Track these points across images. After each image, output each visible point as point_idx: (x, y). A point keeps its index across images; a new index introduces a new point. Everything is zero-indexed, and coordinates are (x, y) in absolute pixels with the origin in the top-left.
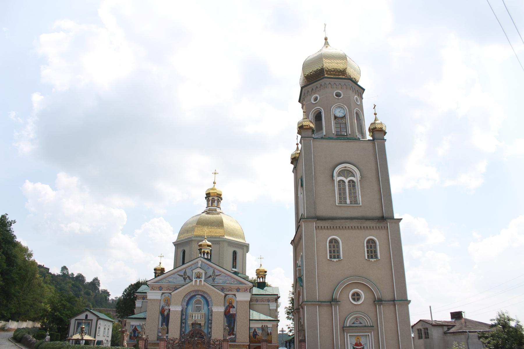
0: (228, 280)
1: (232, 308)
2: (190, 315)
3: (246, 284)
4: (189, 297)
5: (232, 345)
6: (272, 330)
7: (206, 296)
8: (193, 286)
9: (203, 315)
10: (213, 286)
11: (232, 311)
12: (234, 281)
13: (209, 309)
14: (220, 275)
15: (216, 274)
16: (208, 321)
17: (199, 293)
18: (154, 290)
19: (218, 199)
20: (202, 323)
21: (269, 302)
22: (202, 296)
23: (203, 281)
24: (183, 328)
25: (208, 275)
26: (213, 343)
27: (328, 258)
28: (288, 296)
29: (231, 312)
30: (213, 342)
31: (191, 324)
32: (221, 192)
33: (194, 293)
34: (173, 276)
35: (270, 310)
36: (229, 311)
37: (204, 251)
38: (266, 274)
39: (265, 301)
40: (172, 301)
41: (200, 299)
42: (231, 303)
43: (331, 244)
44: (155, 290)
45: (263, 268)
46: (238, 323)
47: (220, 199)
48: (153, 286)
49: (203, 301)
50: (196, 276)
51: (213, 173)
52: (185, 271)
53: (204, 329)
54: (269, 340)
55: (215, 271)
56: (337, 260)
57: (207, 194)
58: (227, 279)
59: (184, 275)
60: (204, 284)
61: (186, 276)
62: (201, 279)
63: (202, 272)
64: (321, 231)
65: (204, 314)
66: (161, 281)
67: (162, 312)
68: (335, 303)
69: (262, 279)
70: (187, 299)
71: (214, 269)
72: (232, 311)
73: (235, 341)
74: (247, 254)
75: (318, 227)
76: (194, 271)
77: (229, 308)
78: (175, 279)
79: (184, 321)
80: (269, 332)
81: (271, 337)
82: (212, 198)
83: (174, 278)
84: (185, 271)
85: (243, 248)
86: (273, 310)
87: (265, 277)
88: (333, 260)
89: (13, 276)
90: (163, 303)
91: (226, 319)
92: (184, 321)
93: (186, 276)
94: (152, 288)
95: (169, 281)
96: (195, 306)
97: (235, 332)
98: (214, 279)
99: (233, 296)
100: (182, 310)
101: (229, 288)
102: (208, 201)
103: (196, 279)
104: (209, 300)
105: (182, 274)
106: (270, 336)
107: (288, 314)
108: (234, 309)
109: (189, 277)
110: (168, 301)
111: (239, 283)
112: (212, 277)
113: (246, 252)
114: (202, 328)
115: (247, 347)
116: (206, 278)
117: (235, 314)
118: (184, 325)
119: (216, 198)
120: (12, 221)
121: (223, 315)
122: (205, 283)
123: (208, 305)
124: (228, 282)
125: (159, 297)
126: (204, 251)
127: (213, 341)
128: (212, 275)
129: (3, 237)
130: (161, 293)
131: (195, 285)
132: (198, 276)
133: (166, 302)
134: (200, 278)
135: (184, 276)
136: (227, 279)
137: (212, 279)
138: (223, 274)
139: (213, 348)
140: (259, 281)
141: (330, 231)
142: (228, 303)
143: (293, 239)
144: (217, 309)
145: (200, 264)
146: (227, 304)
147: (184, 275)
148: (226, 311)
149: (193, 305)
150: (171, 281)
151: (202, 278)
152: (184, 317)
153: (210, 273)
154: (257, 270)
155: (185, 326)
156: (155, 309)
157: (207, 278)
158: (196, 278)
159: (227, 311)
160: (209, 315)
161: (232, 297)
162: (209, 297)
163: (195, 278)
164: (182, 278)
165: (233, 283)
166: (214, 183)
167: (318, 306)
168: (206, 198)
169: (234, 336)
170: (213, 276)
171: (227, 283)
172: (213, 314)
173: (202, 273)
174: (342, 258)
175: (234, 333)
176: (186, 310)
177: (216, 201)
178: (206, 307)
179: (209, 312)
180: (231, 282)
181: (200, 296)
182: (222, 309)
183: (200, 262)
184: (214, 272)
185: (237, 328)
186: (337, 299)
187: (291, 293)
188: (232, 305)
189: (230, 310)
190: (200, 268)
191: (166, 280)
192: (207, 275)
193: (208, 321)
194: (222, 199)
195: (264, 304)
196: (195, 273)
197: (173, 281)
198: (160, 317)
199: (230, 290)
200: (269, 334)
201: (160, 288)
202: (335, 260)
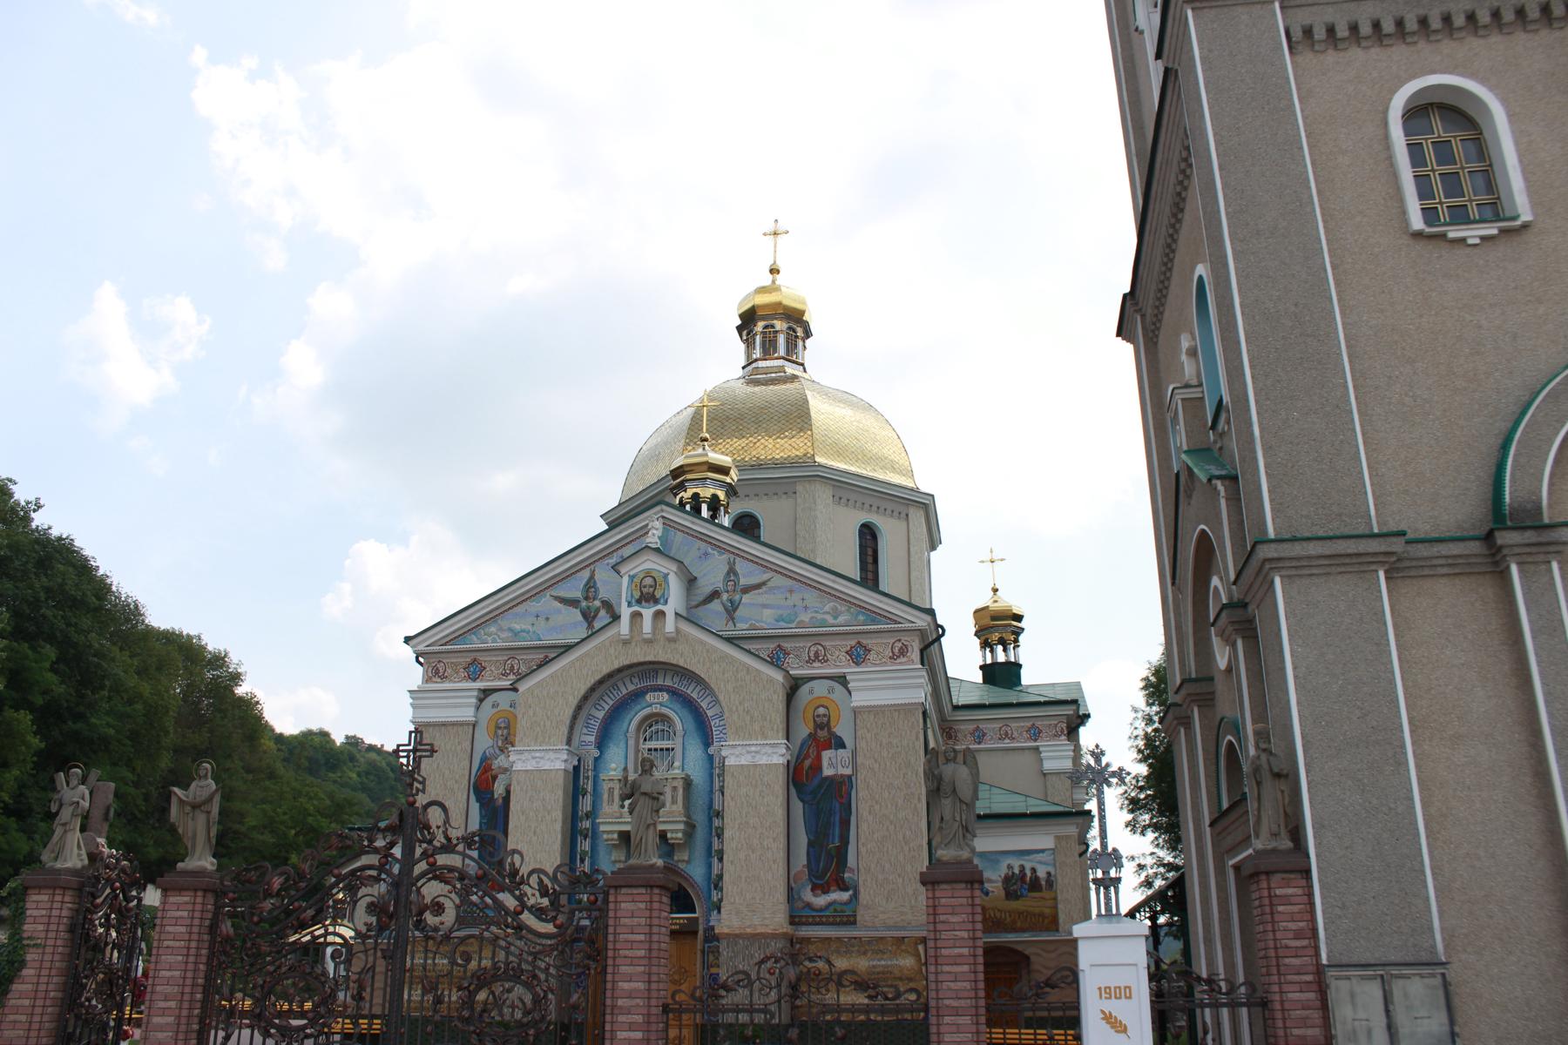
0: (806, 608)
1: (829, 747)
2: (611, 790)
3: (896, 622)
4: (611, 703)
5: (839, 939)
6: (1055, 866)
7: (694, 695)
8: (626, 643)
9: (675, 788)
10: (730, 640)
11: (831, 765)
12: (835, 609)
13: (711, 758)
14: (764, 584)
15: (743, 581)
16: (710, 820)
17: (660, 682)
18: (443, 678)
19: (790, 328)
20: (673, 831)
21: (1035, 740)
22: (673, 692)
23: (670, 618)
24: (582, 861)
25: (705, 587)
26: (545, 902)
27: (1417, 222)
28: (1128, 731)
29: (827, 772)
30: (544, 892)
31: (616, 836)
32: (804, 303)
33: (636, 680)
34: (534, 606)
35: (1045, 775)
36: (817, 767)
37: (696, 496)
38: (1023, 629)
39: (1015, 734)
40: (522, 725)
41: (665, 710)
42: (823, 724)
43: (1416, 139)
44: (451, 681)
45: (1011, 599)
46: (864, 827)
47: (800, 332)
48: (439, 662)
49: (679, 719)
50: (637, 595)
51: (765, 234)
52: (592, 577)
53: (688, 862)
54: (1041, 915)
55: (738, 568)
56: (1491, 230)
57: (742, 316)
58: (799, 603)
59: (586, 598)
60: (678, 630)
61: (597, 603)
62: (660, 607)
63: (666, 571)
64: (1331, 57)
65: (680, 784)
66: (474, 634)
67: (483, 783)
68: (1530, 536)
69: (1005, 650)
70: (601, 715)
71: (732, 557)
72: (831, 765)
73: (851, 921)
74: (932, 554)
75: (1308, 32)
76: (623, 570)
77: (813, 752)
78: (542, 620)
79: (587, 824)
80: (1041, 874)
81: (1055, 899)
82: (766, 327)
83: (537, 616)
84: (592, 577)
85: (907, 515)
86: (1058, 774)
87: (1016, 641)
88: (1454, 233)
89: (93, 720)
90: (484, 742)
91: (798, 807)
92: (587, 824)
93: (597, 603)
94: (437, 672)
95: (516, 634)
96: (641, 746)
97: (852, 870)
98: (731, 610)
99: (838, 687)
100: (576, 769)
101: (813, 649)
102: (749, 343)
103: (636, 608)
104: (710, 713)
105: (578, 594)
106: (1045, 894)
107: (1131, 811)
108: (841, 751)
109: (607, 605)
110: (508, 727)
111: (861, 618)
112: (725, 596)
113: (925, 544)
114: (676, 858)
115: (921, 948)
116: (694, 603)
117: (850, 777)
118: (586, 845)
119: (779, 325)
120: (28, 503)
121: (779, 782)
122: (688, 628)
123: (707, 741)
124: (805, 617)
125: (467, 714)
126: (696, 496)
127: (541, 882)
128: (720, 585)
129: (45, 584)
130: (475, 693)
131: (632, 637)
132: (645, 590)
133: (500, 732)
134: (656, 602)
135: (584, 604)
136: (799, 603)
137: (721, 609)
138: (778, 581)
139: (540, 935)
140: (989, 661)
141: (1399, 53)
142: (811, 724)
143: (1127, 290)
144: (748, 752)
145: (658, 533)
146: (803, 730)
147: (586, 598)
148: (803, 761)
149: (631, 742)
150: (523, 631)
151: (666, 602)
152: (586, 804)
153: (712, 575)
154: (976, 612)
155: (594, 847)
156: (447, 772)
157: (697, 606)
158: (639, 602)
159: (807, 763)
160: (711, 792)
161: (830, 691)
162: (709, 699)
163: (630, 604)
164: (578, 611)
165: (831, 620)
166: (772, 271)
167: (1381, 574)
168: (740, 329)
169: (845, 896)
170: (728, 592)
171: (803, 621)
172: (728, 780)
173: (666, 576)
174: (1526, 216)
175: (846, 875)
176: (595, 768)
177: (781, 339)
178: (695, 753)
179: (711, 775)
180: (819, 616)
181: (665, 696)
182: (774, 755)
183: (658, 524)
184: (732, 571)
185: (863, 850)
186: (1539, 508)
187: (1140, 715)
188: (832, 734)
189: (819, 758)
190: (657, 550)
191: (501, 629)
192: (699, 591)
193: (710, 820)
194: (808, 334)
195: (1014, 749)
196: (632, 578)
197: (530, 627)
198: (475, 807)
199: (817, 654)
200: (1043, 883)
201: (474, 670)
202: (1473, 233)
